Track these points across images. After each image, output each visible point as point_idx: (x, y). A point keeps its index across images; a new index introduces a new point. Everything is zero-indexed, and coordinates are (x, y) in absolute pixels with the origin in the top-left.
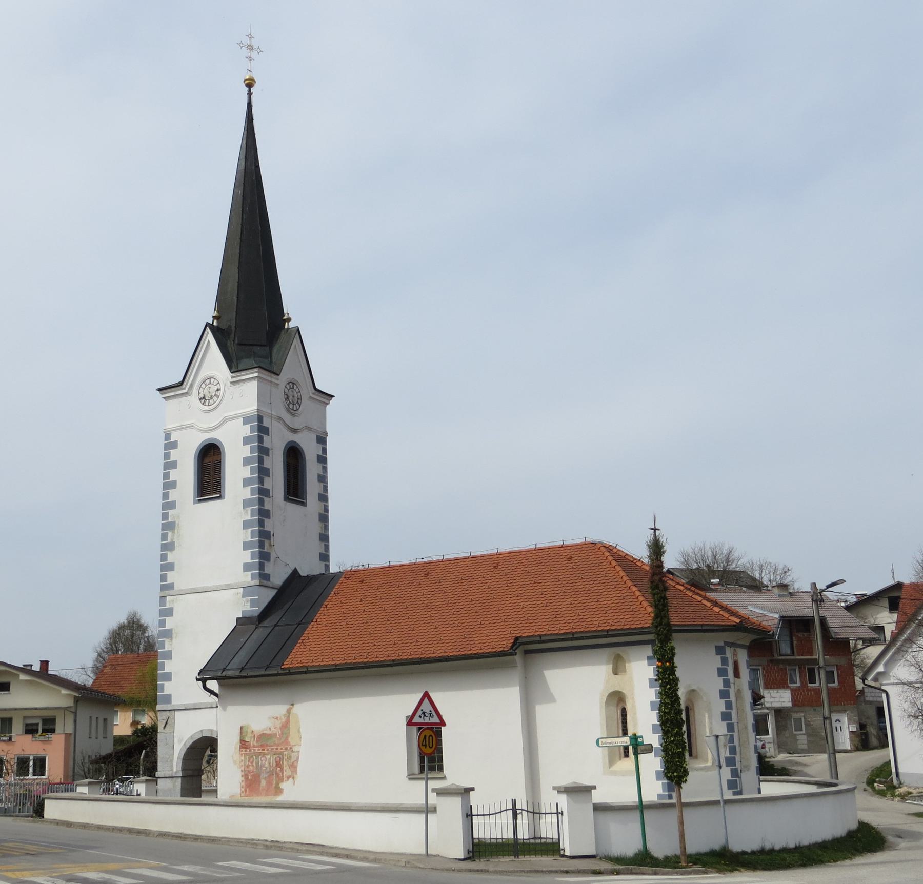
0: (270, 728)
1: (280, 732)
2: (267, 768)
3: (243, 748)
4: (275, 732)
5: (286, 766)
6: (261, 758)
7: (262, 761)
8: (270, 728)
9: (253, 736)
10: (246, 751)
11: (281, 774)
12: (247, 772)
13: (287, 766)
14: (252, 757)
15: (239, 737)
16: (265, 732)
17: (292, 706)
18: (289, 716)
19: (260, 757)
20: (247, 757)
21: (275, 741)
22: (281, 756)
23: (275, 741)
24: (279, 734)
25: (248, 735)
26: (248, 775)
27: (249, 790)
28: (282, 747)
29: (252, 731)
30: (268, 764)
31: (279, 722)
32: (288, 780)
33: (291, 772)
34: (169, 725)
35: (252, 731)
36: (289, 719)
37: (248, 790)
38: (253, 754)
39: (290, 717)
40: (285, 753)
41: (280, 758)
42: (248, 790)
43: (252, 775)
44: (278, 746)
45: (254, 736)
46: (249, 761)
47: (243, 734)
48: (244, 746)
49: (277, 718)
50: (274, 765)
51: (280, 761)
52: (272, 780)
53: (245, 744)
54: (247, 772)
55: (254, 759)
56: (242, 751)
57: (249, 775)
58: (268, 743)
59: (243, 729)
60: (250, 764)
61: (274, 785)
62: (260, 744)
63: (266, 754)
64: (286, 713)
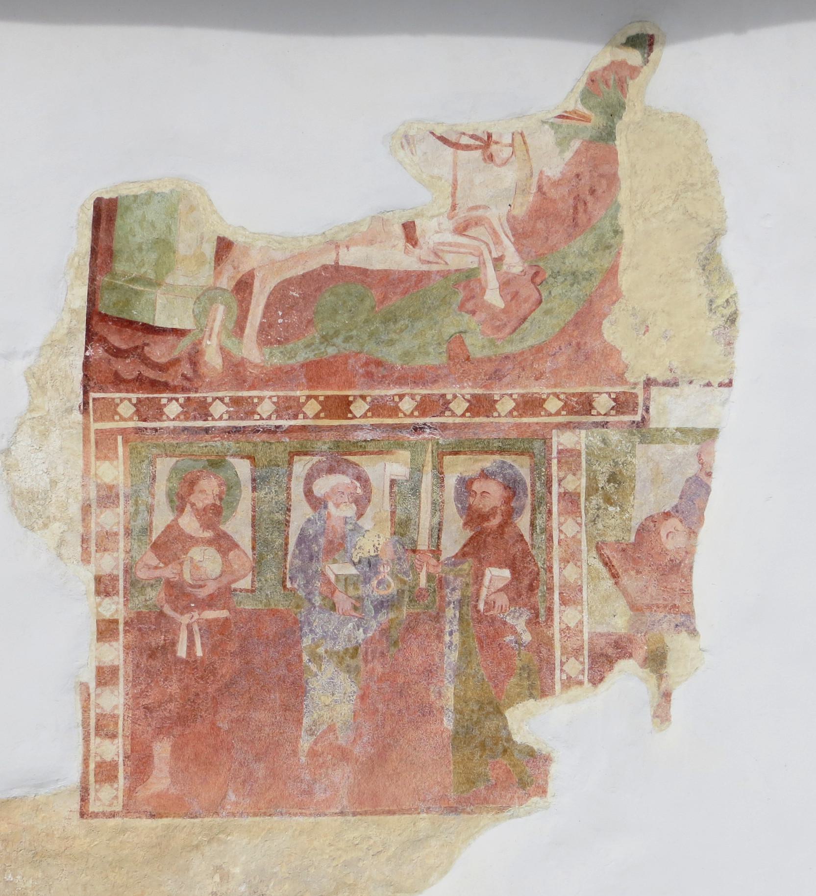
0: (409, 229)
1: (515, 264)
2: (372, 564)
3: (118, 382)
4: (454, 262)
5: (571, 557)
6: (310, 479)
7: (316, 502)
8: (409, 229)
9: (226, 282)
10: (142, 410)
11: (519, 622)
12: (155, 595)
13: (590, 559)
14: (217, 463)
15: (83, 291)
16: (351, 257)
17: (633, 57)
18: (608, 135)
19: (301, 466)
20: (164, 466)
21: (458, 338)
22: (522, 467)
23: (458, 338)
24: (506, 284)
25: (178, 278)
26: (172, 628)
27: (177, 750)
28: (538, 389)
29: (224, 247)
30: (386, 535)
31: (509, 176)
32: (597, 680)
33: (634, 607)
34: (86, 265)
35: (224, 247)
36: (612, 157)
37: (162, 750)
38: (231, 444)
39: (620, 143)
40: (563, 440)
41: (512, 487)
42: (162, 750)
43: (208, 628)
44: (496, 376)
45: (244, 286)
46: (179, 502)
47: (120, 267)
48: (127, 368)
49: (486, 142)
50: (452, 543)
51: (510, 514)
52: (430, 672)
53: (138, 353)
54: (155, 595)
55: (231, 487)
56: (109, 410)
57: (185, 619)
58: (392, 355)
59: (124, 224)
60: (189, 523)
61: (448, 723)
62: (304, 356)
63: (362, 449)
64: (574, 104)
